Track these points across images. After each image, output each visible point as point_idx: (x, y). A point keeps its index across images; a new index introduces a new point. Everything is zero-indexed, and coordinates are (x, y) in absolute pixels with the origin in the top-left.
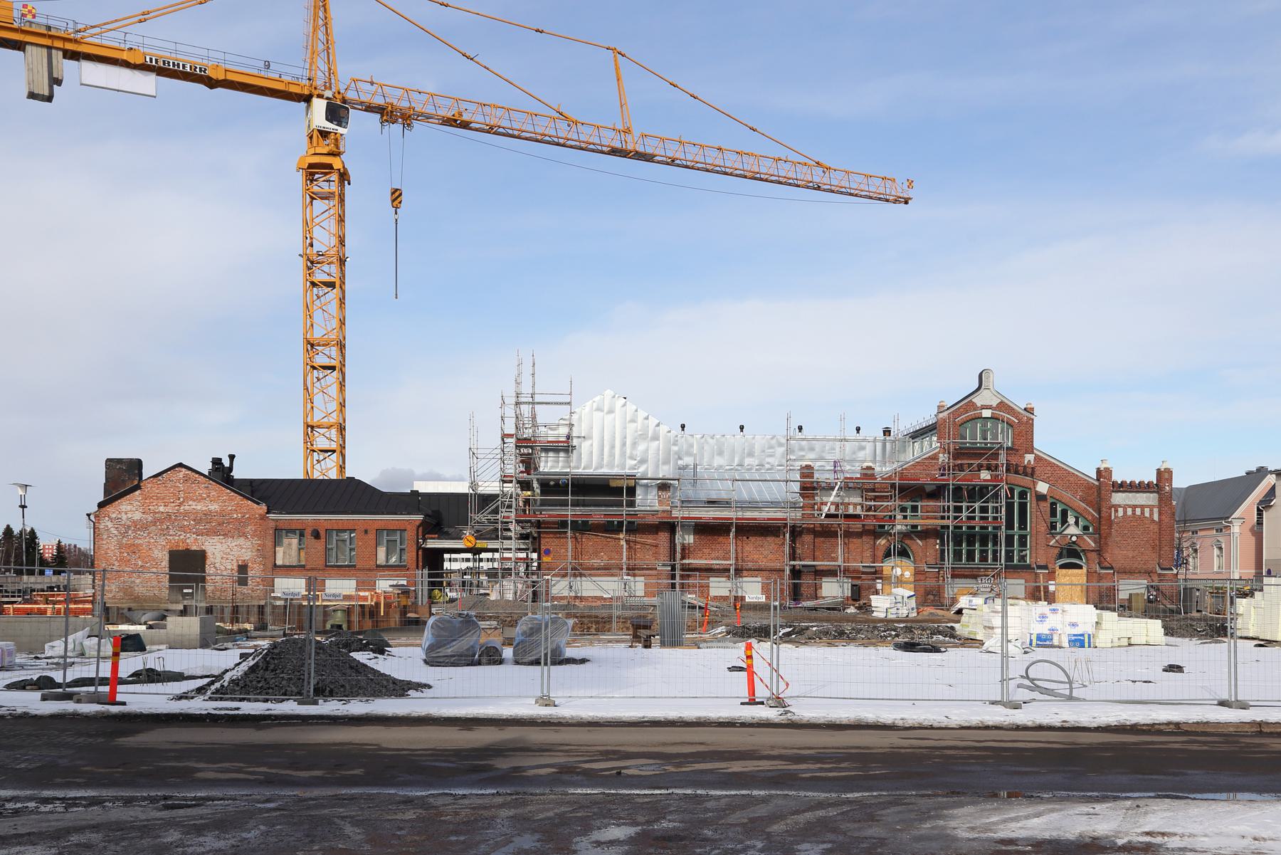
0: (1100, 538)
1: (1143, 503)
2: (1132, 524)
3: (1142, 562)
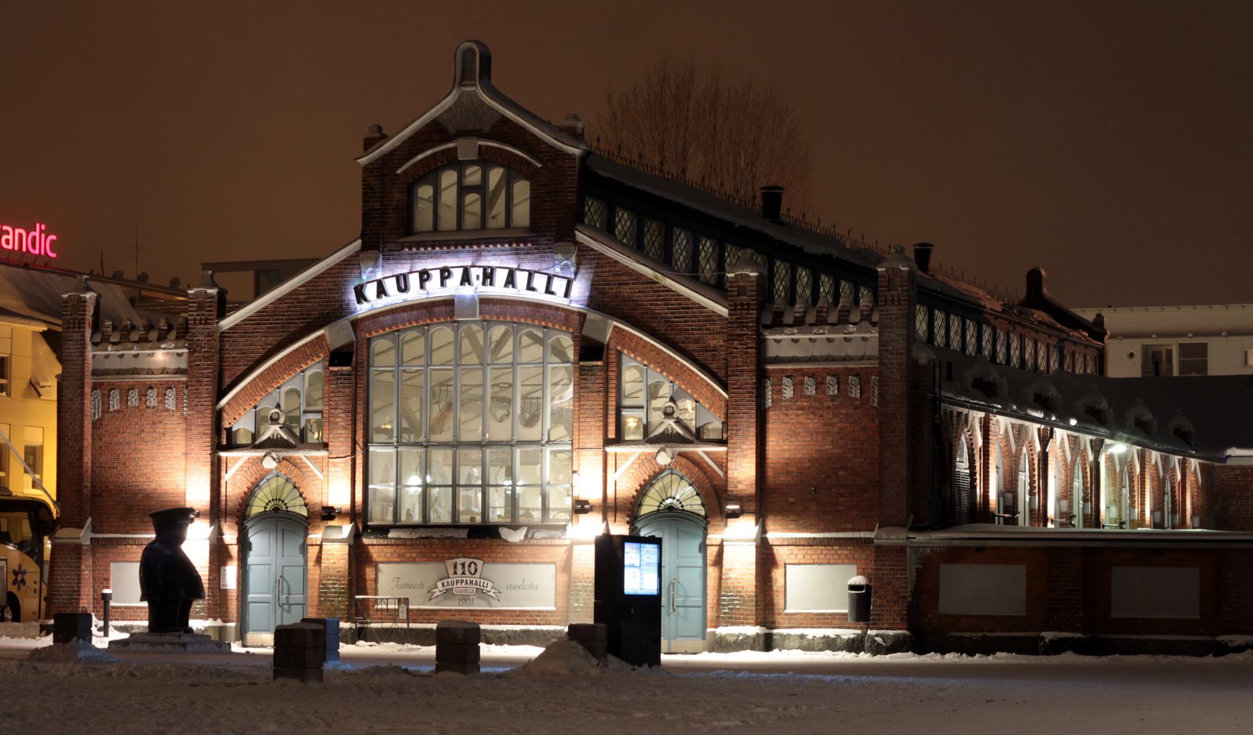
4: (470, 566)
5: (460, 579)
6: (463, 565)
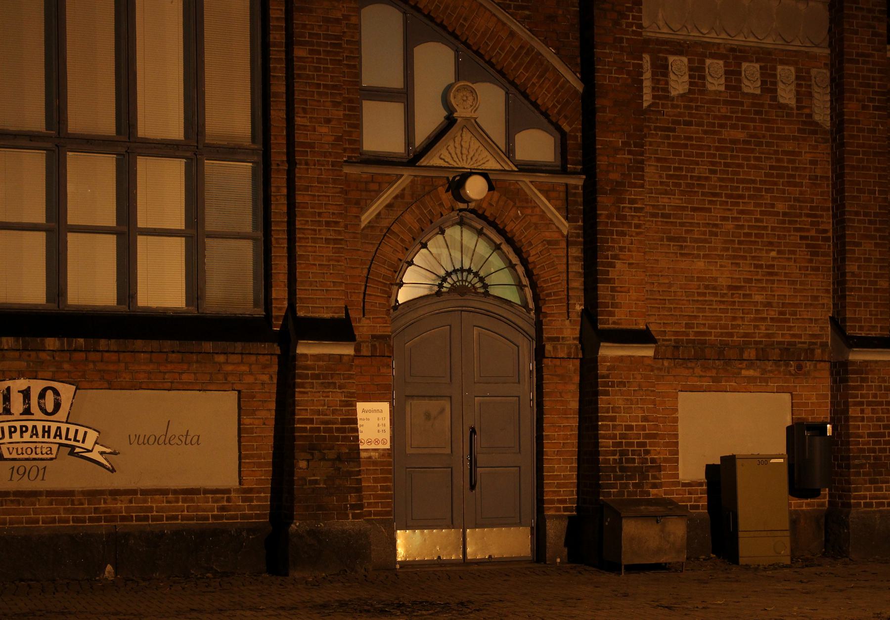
0: (591, 191)
1: (769, 42)
2: (728, 134)
3: (773, 314)
4: (42, 395)
5: (18, 424)
6: (26, 394)
